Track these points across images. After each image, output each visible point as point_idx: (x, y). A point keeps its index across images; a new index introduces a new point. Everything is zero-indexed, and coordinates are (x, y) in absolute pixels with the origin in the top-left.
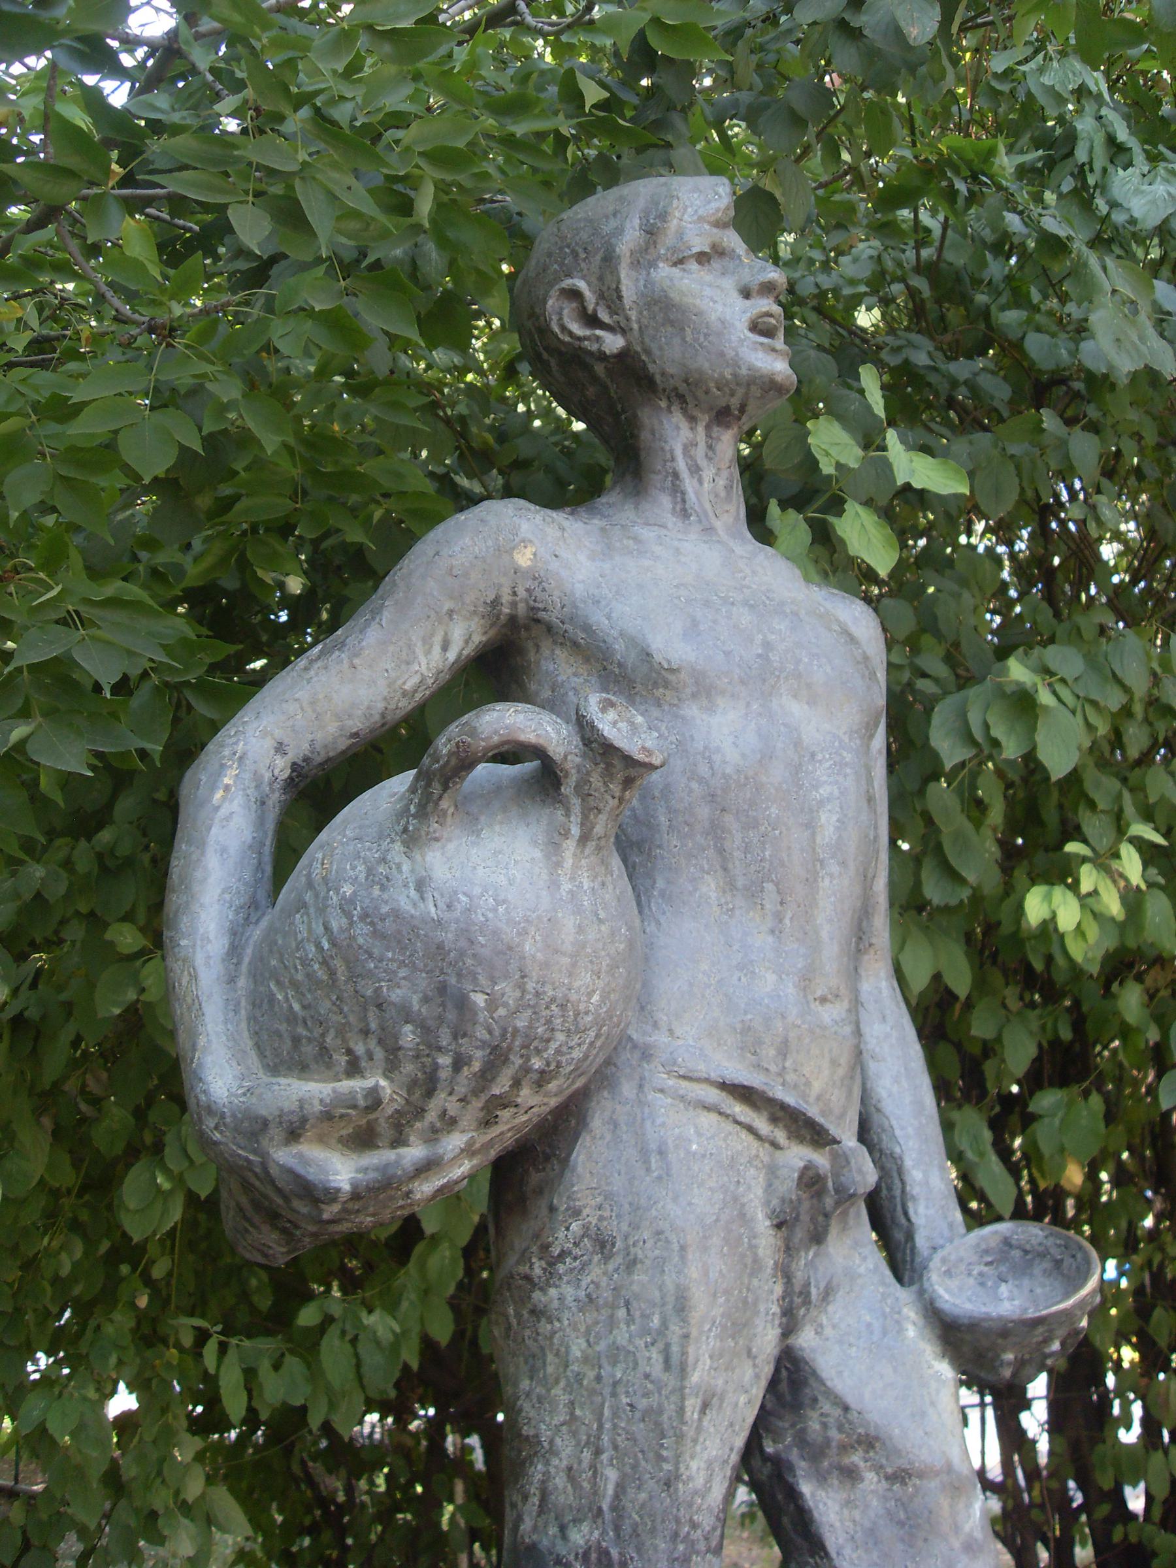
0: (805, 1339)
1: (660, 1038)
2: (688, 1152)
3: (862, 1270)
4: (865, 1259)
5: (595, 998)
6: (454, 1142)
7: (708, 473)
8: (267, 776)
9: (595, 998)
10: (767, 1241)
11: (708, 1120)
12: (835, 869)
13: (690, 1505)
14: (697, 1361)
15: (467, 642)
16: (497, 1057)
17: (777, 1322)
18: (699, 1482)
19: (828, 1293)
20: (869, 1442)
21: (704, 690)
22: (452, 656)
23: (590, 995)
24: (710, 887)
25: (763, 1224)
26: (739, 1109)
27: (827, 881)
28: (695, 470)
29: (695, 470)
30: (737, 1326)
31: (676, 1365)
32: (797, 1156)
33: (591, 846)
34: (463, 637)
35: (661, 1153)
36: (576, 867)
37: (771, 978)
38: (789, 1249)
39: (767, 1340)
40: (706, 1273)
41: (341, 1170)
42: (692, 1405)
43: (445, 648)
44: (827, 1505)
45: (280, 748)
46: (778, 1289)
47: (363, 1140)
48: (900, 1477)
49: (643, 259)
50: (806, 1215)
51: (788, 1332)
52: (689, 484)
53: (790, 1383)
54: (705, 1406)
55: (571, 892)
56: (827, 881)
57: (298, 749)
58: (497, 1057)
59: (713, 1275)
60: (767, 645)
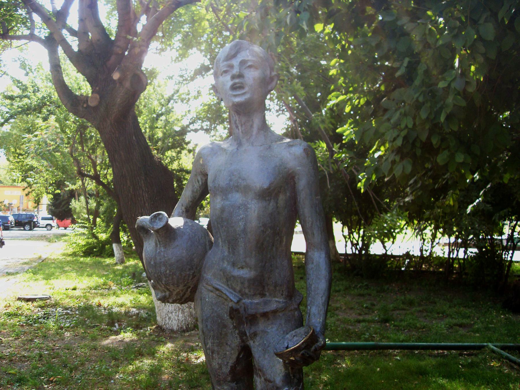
0: (251, 343)
1: (205, 275)
2: (205, 300)
3: (269, 331)
4: (272, 328)
5: (168, 272)
7: (240, 128)
8: (181, 211)
9: (168, 272)
11: (211, 294)
12: (244, 236)
13: (216, 371)
14: (208, 343)
15: (202, 179)
17: (238, 338)
18: (217, 367)
19: (255, 334)
20: (260, 370)
22: (200, 183)
23: (166, 271)
25: (226, 316)
26: (217, 292)
27: (241, 239)
28: (237, 127)
29: (237, 127)
33: (161, 243)
35: (201, 300)
36: (160, 247)
37: (226, 263)
40: (207, 326)
43: (198, 182)
45: (182, 205)
46: (237, 331)
51: (243, 341)
53: (246, 353)
54: (213, 353)
55: (159, 252)
56: (241, 239)
59: (209, 327)
60: (231, 180)
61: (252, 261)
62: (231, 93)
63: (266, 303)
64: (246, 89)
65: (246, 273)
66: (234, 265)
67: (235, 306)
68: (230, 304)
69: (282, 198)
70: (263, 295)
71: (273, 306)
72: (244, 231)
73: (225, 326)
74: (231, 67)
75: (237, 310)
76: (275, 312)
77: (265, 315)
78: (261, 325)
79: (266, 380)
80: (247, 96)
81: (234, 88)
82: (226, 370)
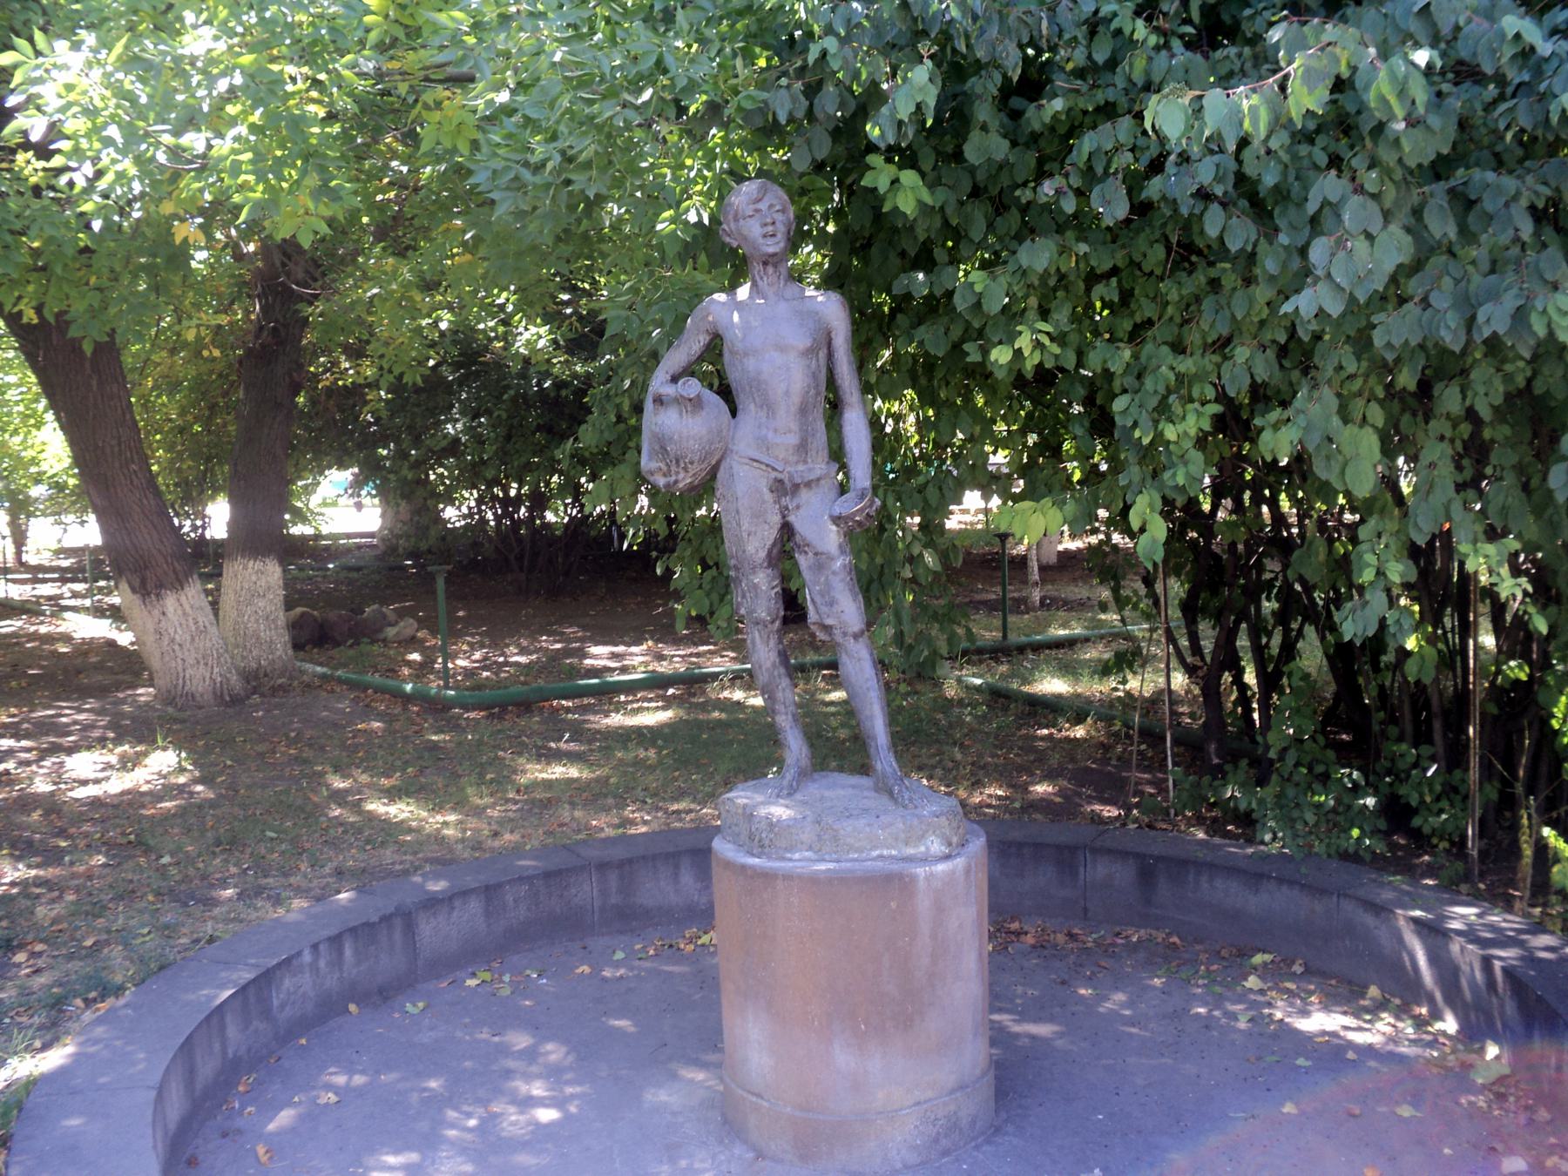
0: (791, 518)
6: (681, 476)
10: (768, 497)
16: (677, 462)
19: (798, 507)
21: (746, 354)
24: (752, 406)
25: (766, 490)
30: (758, 516)
31: (739, 525)
32: (774, 474)
34: (704, 339)
38: (779, 498)
39: (776, 520)
41: (661, 481)
42: (745, 535)
44: (803, 561)
47: (664, 475)
48: (816, 554)
49: (736, 220)
50: (783, 488)
52: (760, 283)
57: (671, 372)
58: (677, 462)
61: (794, 426)
62: (761, 241)
63: (810, 470)
64: (779, 236)
65: (793, 439)
66: (776, 431)
67: (780, 476)
68: (774, 474)
69: (822, 354)
70: (805, 462)
71: (818, 473)
72: (787, 393)
73: (764, 502)
74: (757, 211)
75: (781, 481)
76: (818, 480)
77: (808, 484)
78: (804, 494)
79: (816, 554)
80: (782, 245)
81: (765, 236)
82: (763, 554)
